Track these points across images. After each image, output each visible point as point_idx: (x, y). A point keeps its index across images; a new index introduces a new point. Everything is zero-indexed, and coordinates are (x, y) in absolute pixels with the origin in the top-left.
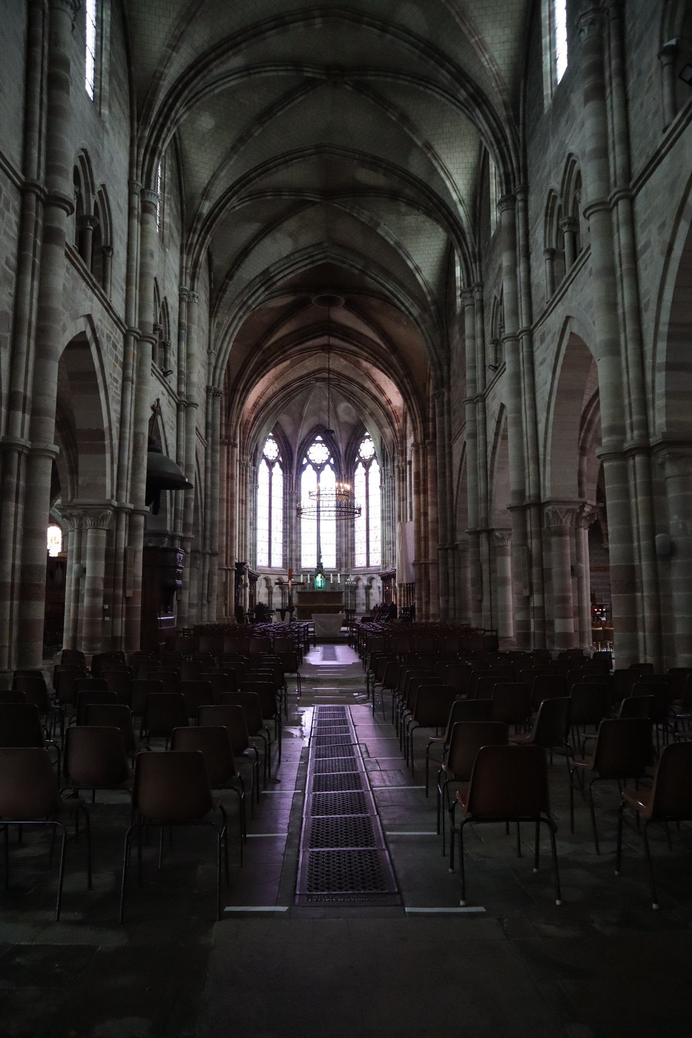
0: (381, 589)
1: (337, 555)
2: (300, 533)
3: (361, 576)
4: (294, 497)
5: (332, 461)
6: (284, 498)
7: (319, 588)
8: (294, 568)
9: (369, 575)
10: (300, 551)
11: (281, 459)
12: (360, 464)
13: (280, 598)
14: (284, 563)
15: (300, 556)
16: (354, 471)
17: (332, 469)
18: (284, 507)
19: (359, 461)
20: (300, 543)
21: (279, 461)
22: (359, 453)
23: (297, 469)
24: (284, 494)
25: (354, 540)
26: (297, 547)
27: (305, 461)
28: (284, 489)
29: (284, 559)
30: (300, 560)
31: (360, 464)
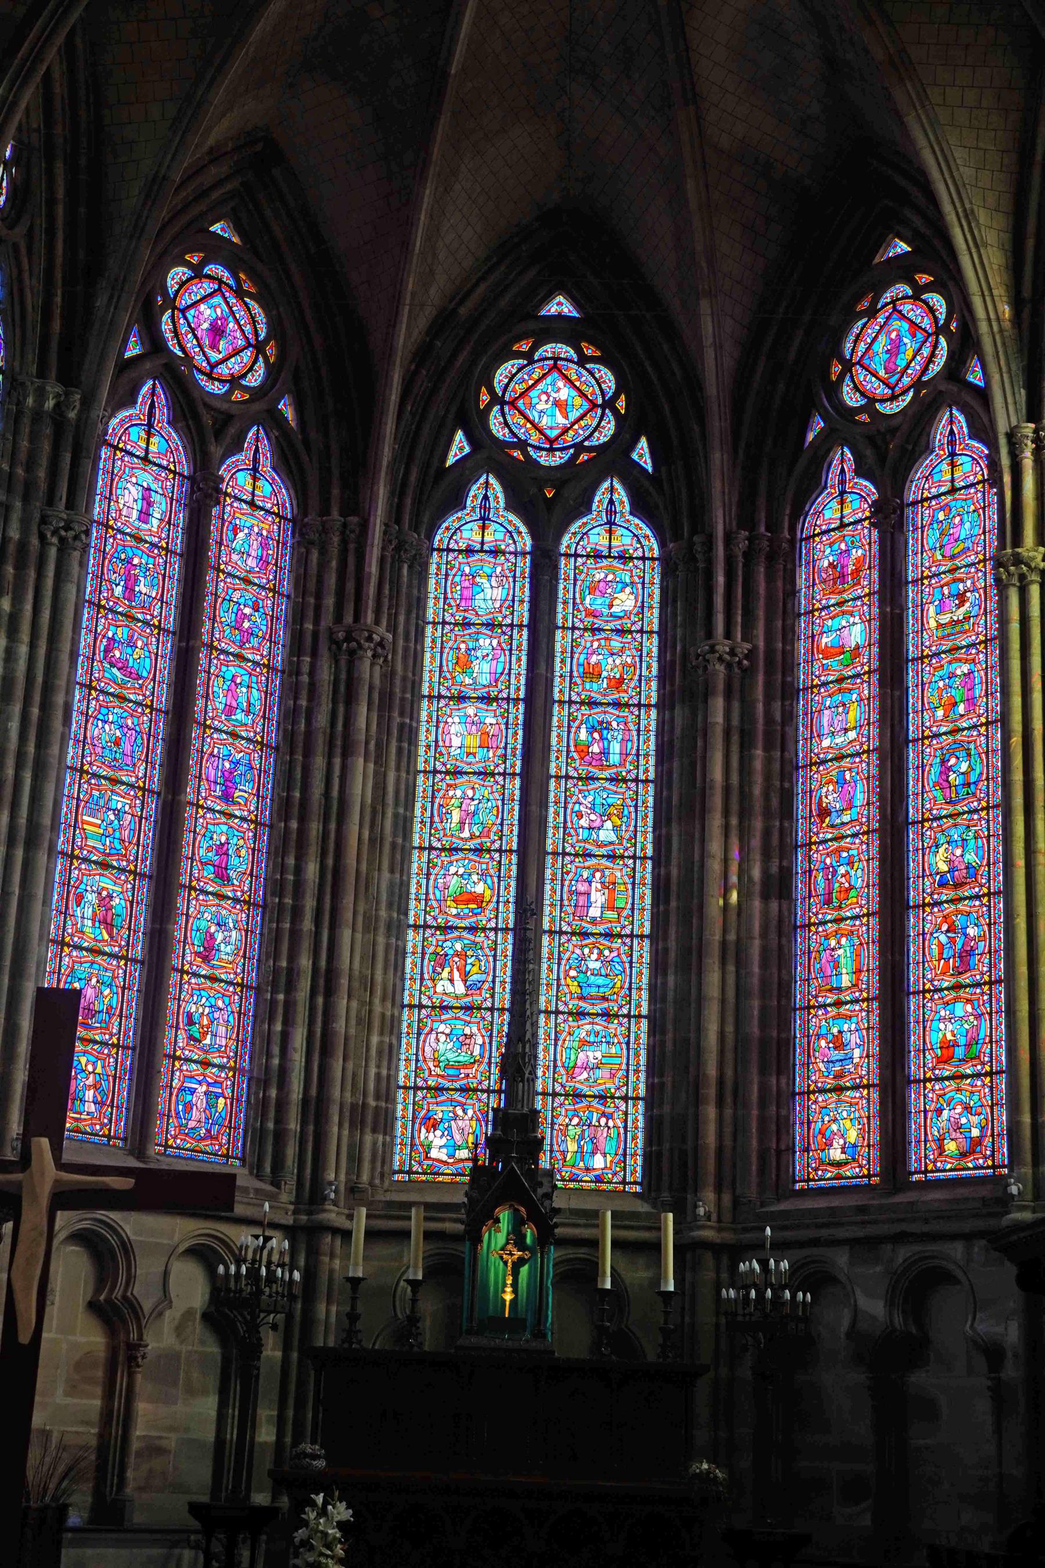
0: (1011, 1371)
1: (653, 1099)
2: (397, 928)
3: (841, 1259)
4: (368, 671)
5: (642, 453)
6: (292, 671)
7: (498, 1323)
8: (335, 1174)
9: (903, 1253)
10: (390, 1054)
11: (287, 409)
12: (843, 459)
13: (209, 1405)
14: (256, 1136)
15: (387, 1091)
16: (799, 511)
17: (641, 507)
18: (289, 737)
19: (828, 441)
20: (394, 995)
21: (273, 420)
22: (834, 389)
23: (398, 492)
24: (296, 645)
25: (785, 989)
26: (365, 1023)
27: (459, 446)
28: (298, 616)
29: (258, 1108)
30: (384, 1122)
31: (843, 459)
